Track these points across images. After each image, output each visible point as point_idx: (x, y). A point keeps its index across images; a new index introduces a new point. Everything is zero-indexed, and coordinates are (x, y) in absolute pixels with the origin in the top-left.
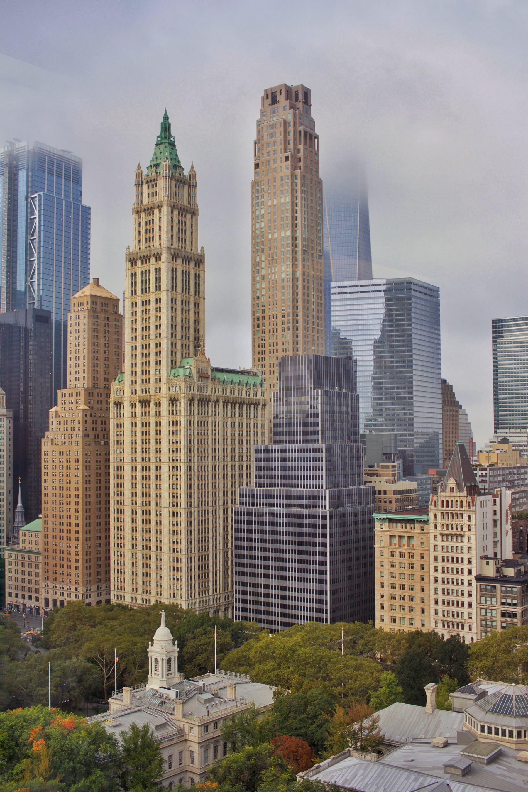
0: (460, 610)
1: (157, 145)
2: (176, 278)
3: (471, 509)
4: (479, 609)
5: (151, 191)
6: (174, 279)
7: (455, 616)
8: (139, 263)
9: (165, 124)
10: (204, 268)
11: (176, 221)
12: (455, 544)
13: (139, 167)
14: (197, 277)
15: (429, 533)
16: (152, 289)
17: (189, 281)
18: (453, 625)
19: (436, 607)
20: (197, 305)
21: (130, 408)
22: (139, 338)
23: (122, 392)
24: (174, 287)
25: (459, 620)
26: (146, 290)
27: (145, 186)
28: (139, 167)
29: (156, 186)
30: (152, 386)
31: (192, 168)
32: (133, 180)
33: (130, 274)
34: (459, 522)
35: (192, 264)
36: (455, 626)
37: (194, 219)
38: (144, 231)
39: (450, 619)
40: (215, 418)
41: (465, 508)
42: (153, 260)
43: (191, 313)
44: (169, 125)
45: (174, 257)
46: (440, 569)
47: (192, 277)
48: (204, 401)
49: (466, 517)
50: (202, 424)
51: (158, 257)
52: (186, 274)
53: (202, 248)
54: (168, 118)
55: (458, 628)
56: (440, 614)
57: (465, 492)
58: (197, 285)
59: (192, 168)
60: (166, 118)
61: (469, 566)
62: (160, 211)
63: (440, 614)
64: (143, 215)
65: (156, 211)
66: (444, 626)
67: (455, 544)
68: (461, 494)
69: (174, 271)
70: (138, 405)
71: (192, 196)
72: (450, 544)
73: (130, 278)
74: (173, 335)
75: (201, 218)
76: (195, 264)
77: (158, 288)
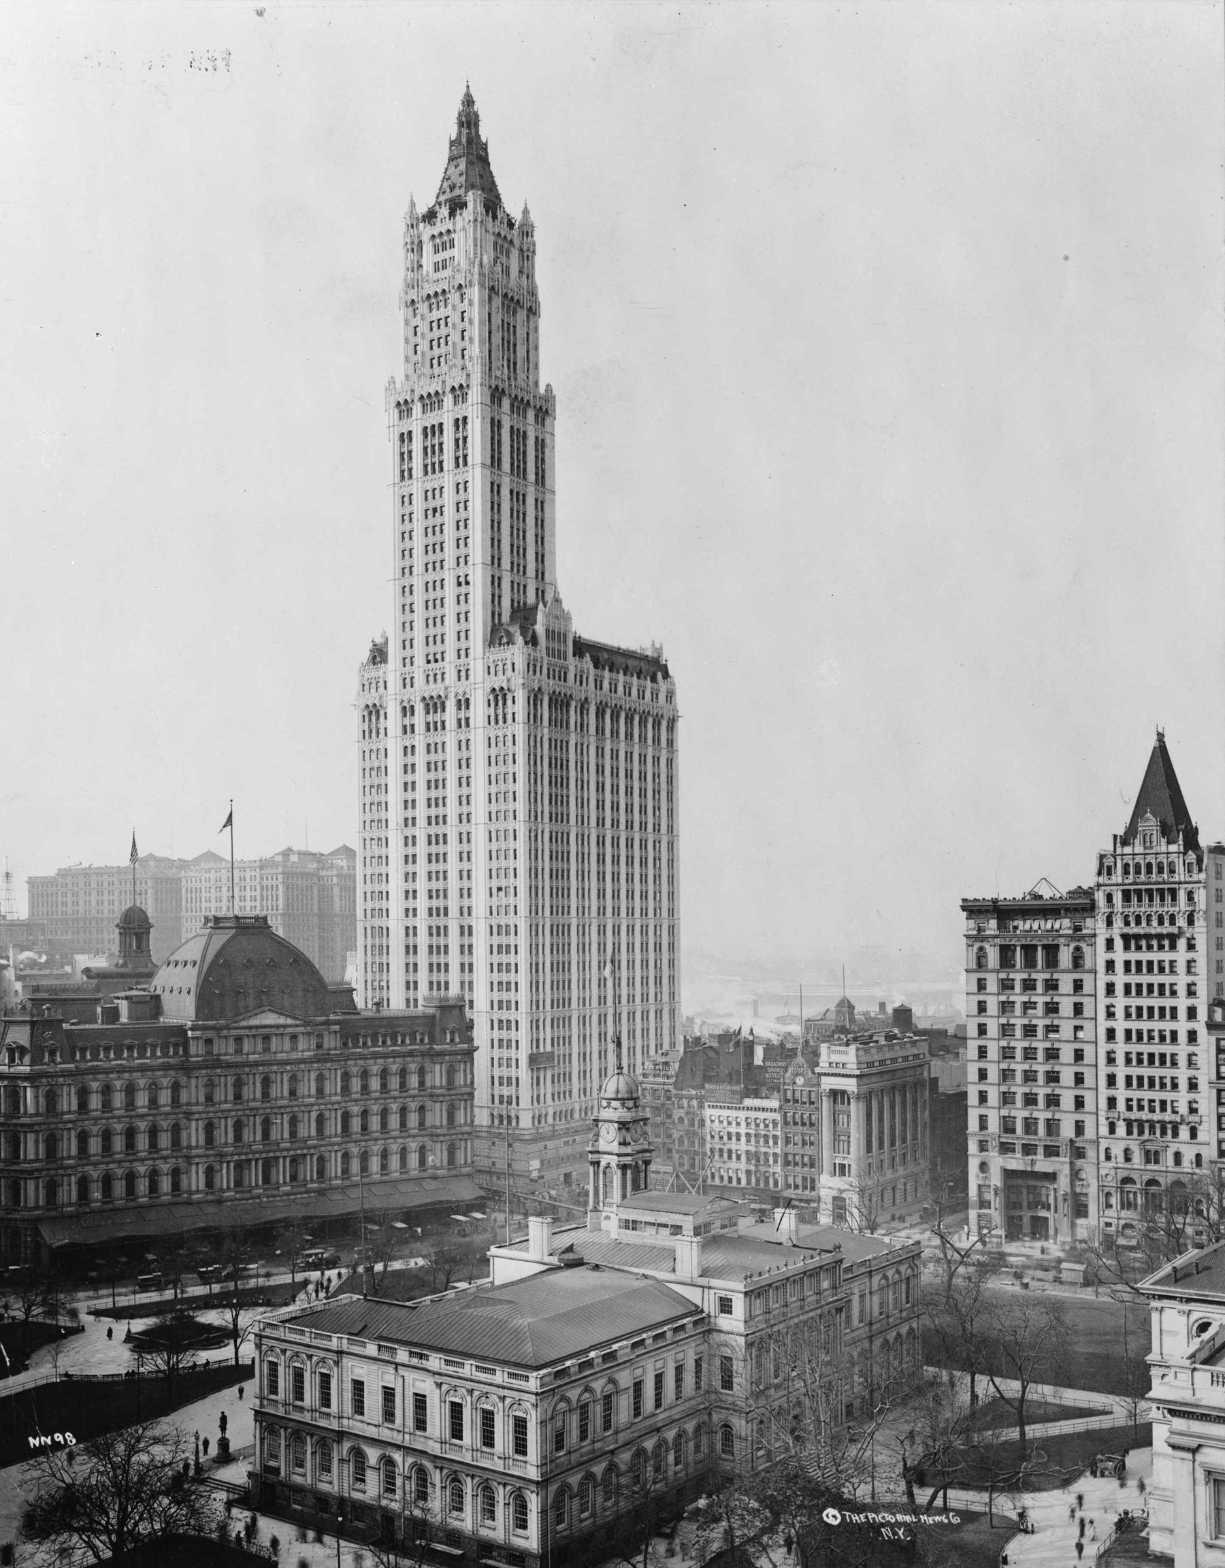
0: (1168, 1096)
2: (499, 441)
3: (1195, 877)
4: (1214, 1092)
5: (440, 257)
7: (1158, 1109)
8: (417, 408)
9: (467, 115)
10: (553, 426)
11: (497, 320)
12: (1155, 956)
14: (541, 445)
15: (1094, 935)
16: (449, 464)
17: (525, 452)
18: (1152, 1128)
19: (1112, 1092)
20: (540, 505)
21: (399, 714)
22: (418, 568)
23: (381, 684)
24: (495, 461)
25: (1168, 1116)
29: (452, 246)
30: (449, 666)
31: (526, 212)
33: (397, 437)
34: (1167, 908)
35: (531, 414)
36: (1158, 1132)
37: (531, 323)
39: (1145, 1115)
40: (582, 737)
41: (1181, 874)
42: (448, 400)
43: (528, 519)
44: (477, 116)
45: (496, 395)
46: (1120, 1012)
47: (531, 442)
48: (560, 703)
49: (1182, 895)
50: (559, 745)
52: (518, 436)
53: (548, 385)
55: (1164, 1133)
56: (1121, 1105)
57: (1181, 842)
58: (541, 460)
60: (469, 101)
61: (1191, 1002)
63: (1121, 1105)
64: (423, 308)
66: (1129, 1132)
67: (1155, 956)
68: (1173, 848)
69: (495, 425)
70: (419, 708)
71: (527, 272)
72: (1144, 956)
73: (397, 443)
74: (495, 561)
75: (545, 322)
76: (537, 416)
77: (461, 461)
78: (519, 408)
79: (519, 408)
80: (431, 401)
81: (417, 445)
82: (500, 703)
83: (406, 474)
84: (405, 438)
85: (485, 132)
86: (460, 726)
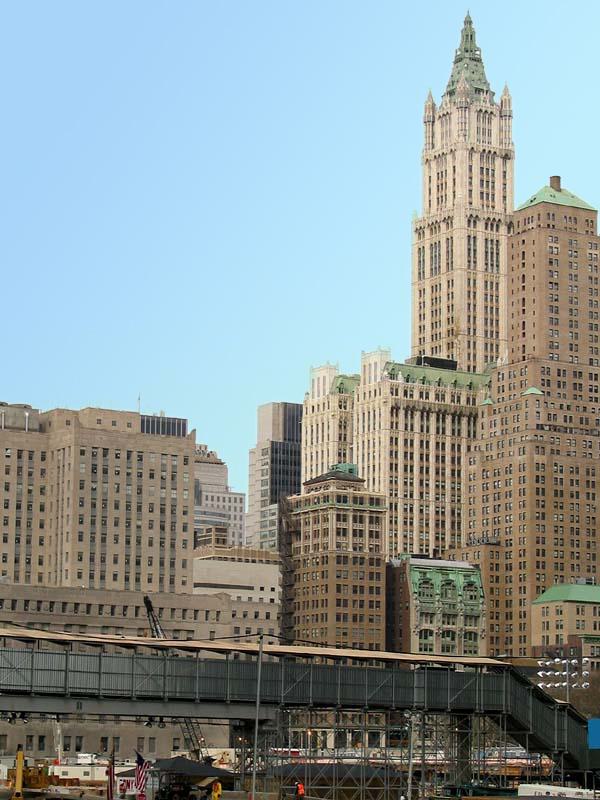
1: (456, 62)
6: (471, 252)
8: (427, 232)
13: (430, 96)
26: (435, 270)
27: (438, 123)
28: (430, 96)
31: (506, 91)
32: (421, 114)
33: (417, 250)
37: (508, 165)
38: (436, 186)
42: (443, 226)
51: (449, 221)
54: (471, 22)
59: (506, 91)
60: (468, 22)
62: (454, 158)
64: (433, 164)
65: (449, 157)
78: (492, 225)
79: (492, 225)
80: (434, 227)
81: (428, 252)
82: (472, 424)
83: (421, 275)
84: (421, 251)
85: (479, 42)
86: (422, 431)
